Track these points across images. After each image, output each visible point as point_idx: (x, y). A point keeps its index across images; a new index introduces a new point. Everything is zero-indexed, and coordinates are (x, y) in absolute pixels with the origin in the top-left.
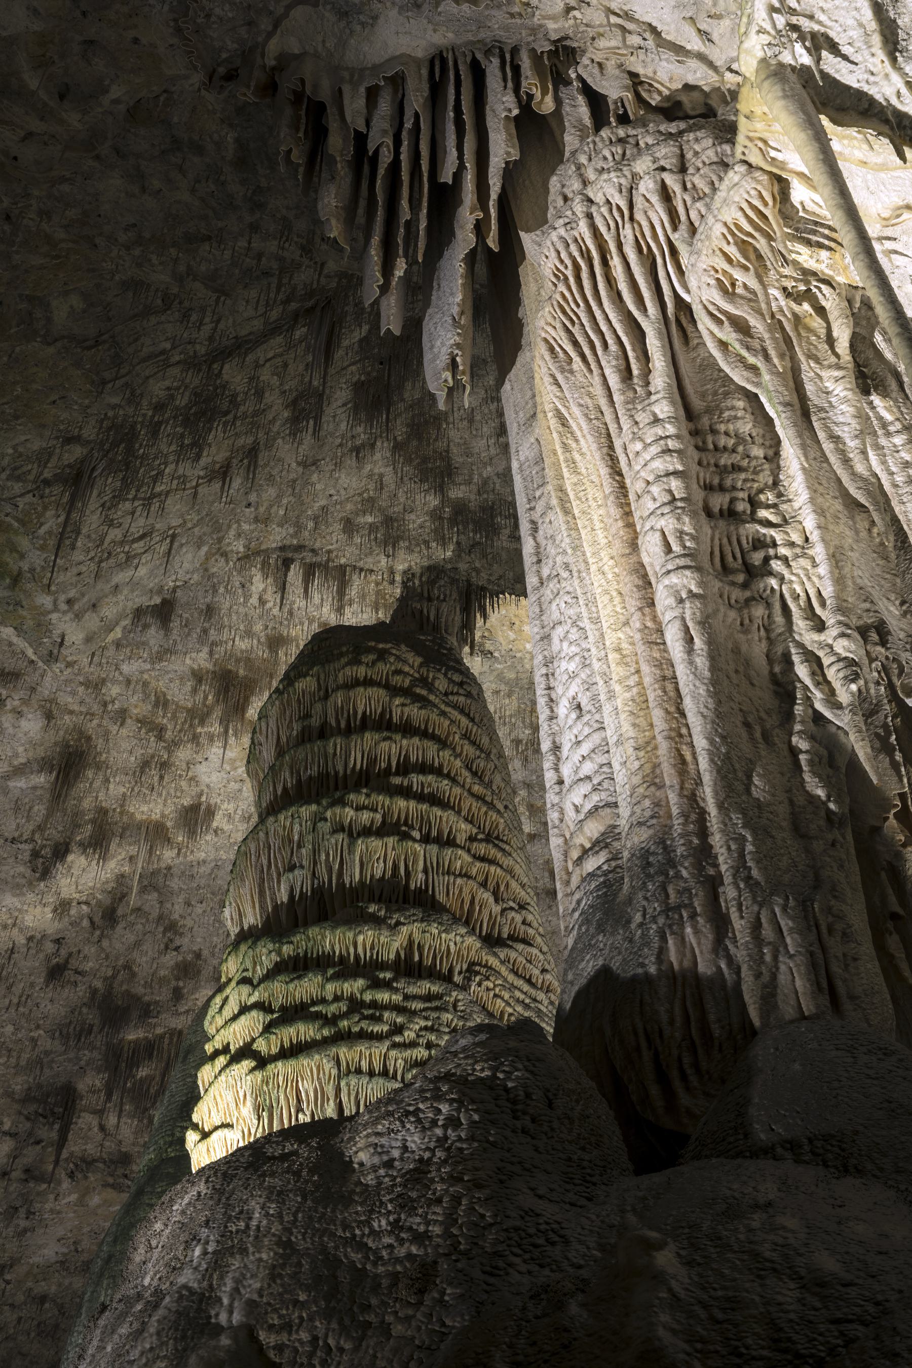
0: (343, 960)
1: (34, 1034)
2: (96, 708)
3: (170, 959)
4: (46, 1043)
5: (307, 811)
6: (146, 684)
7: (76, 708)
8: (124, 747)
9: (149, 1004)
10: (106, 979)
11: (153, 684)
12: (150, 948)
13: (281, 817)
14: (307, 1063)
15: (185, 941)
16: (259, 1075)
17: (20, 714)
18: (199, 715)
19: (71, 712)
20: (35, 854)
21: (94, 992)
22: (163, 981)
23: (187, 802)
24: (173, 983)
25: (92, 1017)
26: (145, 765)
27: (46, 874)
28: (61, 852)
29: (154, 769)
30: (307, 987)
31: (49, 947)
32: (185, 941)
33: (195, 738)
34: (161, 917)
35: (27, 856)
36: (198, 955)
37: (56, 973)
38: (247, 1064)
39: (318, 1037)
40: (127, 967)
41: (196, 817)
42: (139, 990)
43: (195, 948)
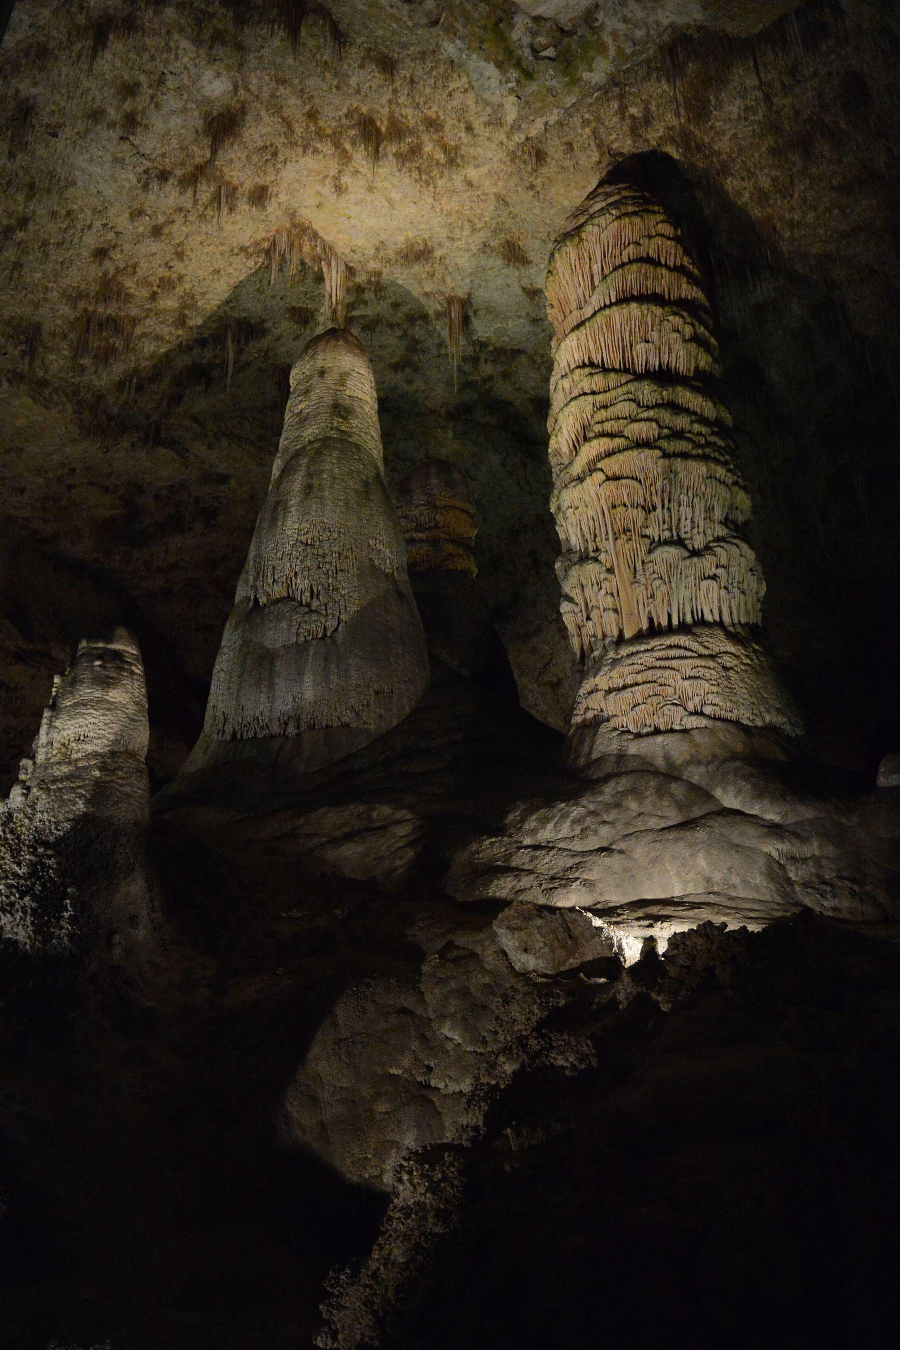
0: (695, 413)
1: (50, 286)
2: (266, 95)
3: (163, 272)
4: (54, 295)
5: (658, 311)
6: (311, 98)
7: (252, 88)
8: (260, 130)
9: (127, 295)
10: (117, 269)
11: (317, 100)
12: (158, 260)
13: (644, 307)
14: (693, 465)
15: (179, 267)
16: (667, 461)
17: (219, 75)
18: (320, 135)
19: (249, 90)
20: (146, 172)
21: (106, 274)
22: (150, 284)
23: (260, 182)
24: (156, 289)
25: (95, 288)
26: (265, 148)
27: (146, 187)
28: (164, 176)
29: (270, 153)
30: (682, 422)
31: (111, 236)
32: (179, 267)
33: (305, 148)
34: (179, 245)
35: (140, 170)
36: (181, 278)
37: (101, 254)
38: (658, 453)
39: (712, 455)
40: (135, 266)
41: (260, 196)
42: (129, 284)
43: (183, 272)
